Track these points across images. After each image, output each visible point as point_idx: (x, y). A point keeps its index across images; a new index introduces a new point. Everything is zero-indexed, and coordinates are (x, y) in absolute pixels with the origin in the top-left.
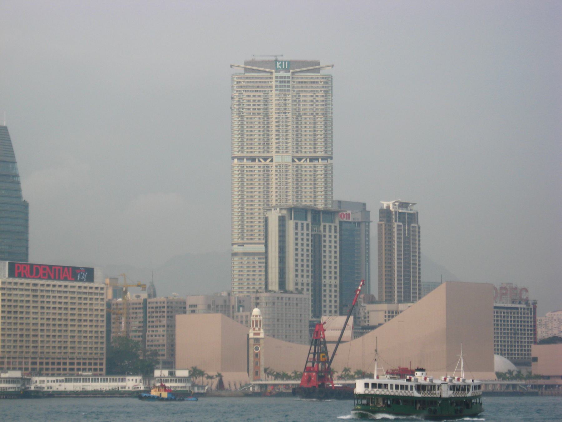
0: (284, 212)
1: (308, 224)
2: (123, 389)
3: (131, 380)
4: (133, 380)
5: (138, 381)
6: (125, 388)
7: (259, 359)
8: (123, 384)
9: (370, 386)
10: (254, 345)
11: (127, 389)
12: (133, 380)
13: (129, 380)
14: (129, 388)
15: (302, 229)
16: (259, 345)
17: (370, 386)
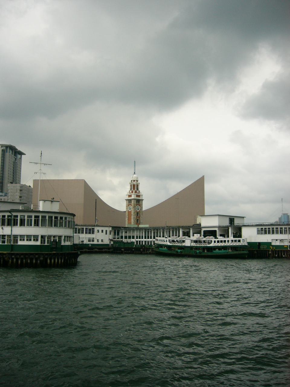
0: (5, 148)
1: (13, 157)
2: (91, 243)
3: (100, 231)
4: (102, 231)
5: (108, 232)
6: (93, 241)
7: (139, 217)
8: (91, 236)
9: (216, 242)
10: (137, 205)
11: (95, 242)
12: (102, 231)
13: (98, 231)
14: (98, 241)
15: (11, 159)
16: (139, 205)
17: (216, 242)
